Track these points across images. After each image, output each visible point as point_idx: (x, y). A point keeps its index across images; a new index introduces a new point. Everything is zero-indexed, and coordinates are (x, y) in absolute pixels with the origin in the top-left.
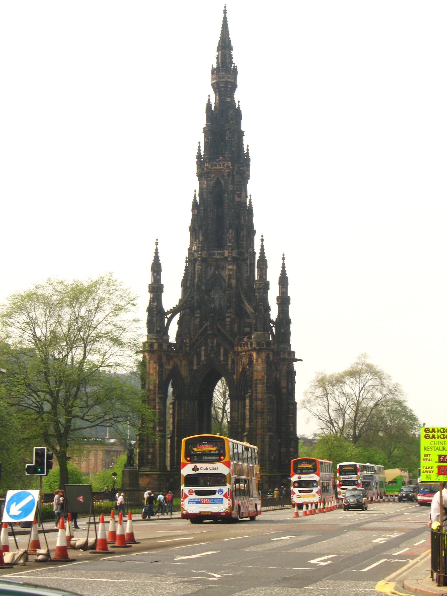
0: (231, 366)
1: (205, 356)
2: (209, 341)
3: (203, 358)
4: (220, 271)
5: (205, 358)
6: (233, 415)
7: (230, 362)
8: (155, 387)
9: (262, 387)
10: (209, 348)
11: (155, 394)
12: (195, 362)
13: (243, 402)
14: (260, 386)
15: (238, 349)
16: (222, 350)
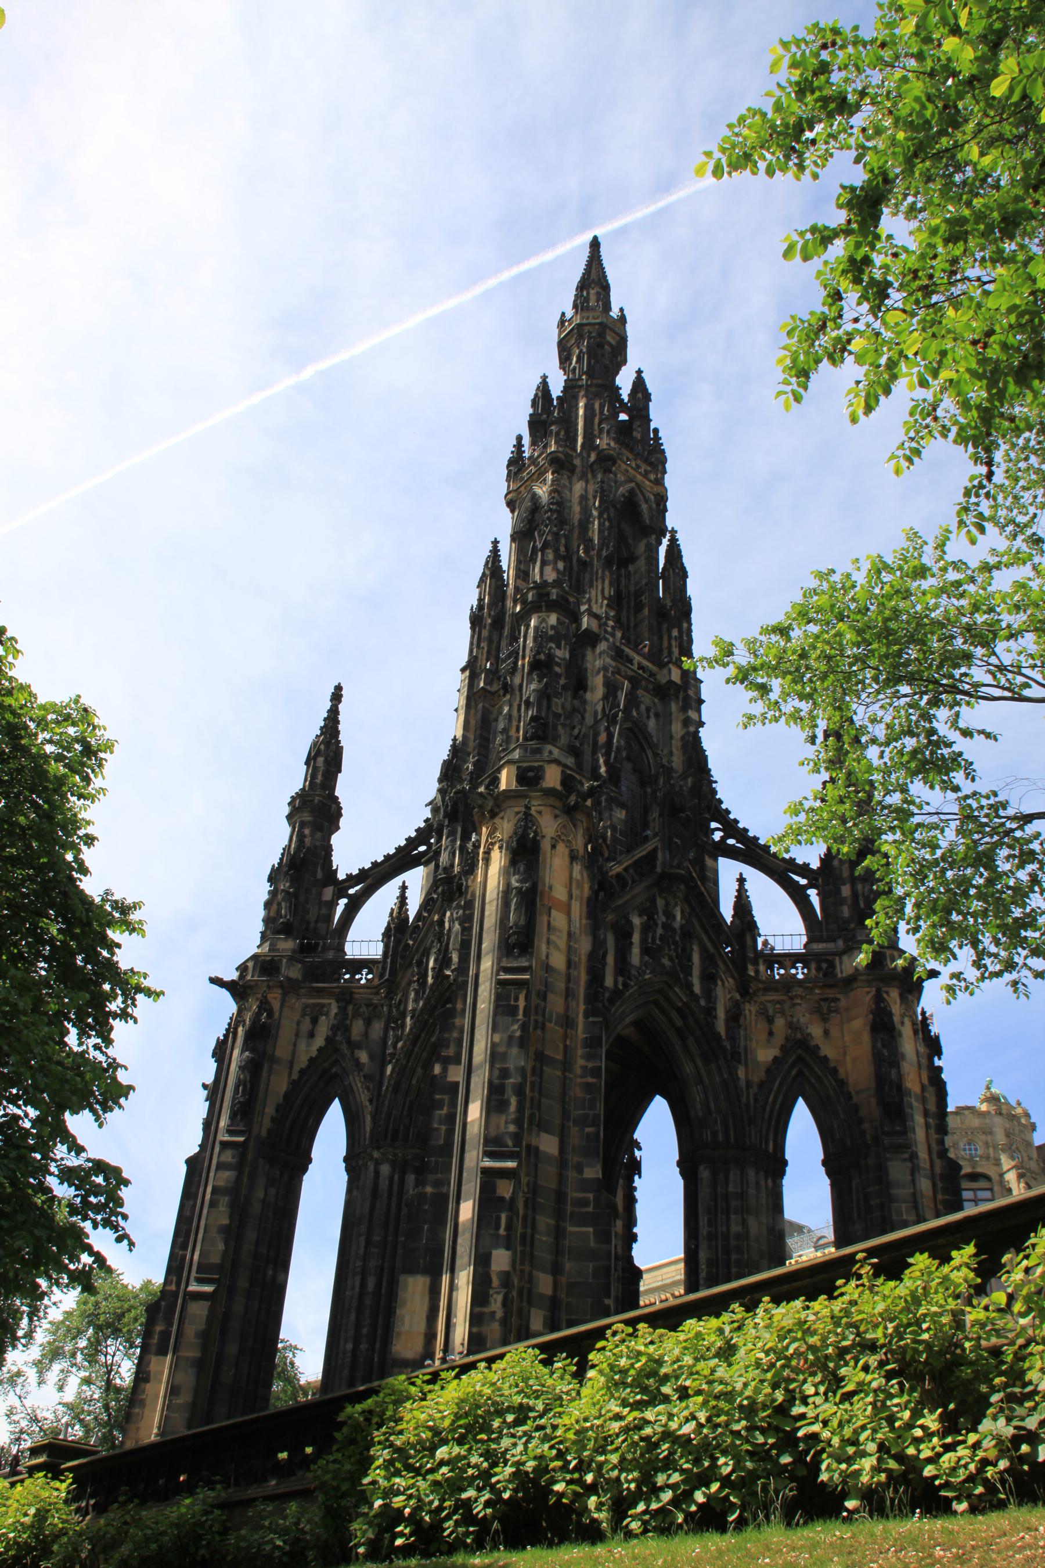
0: (728, 1028)
1: (645, 950)
2: (660, 903)
3: (635, 956)
4: (644, 719)
5: (647, 958)
6: (735, 1228)
7: (721, 1013)
8: (569, 964)
9: (927, 1126)
10: (660, 931)
11: (569, 994)
12: (610, 960)
13: (770, 1182)
14: (919, 1119)
15: (757, 972)
16: (696, 958)
